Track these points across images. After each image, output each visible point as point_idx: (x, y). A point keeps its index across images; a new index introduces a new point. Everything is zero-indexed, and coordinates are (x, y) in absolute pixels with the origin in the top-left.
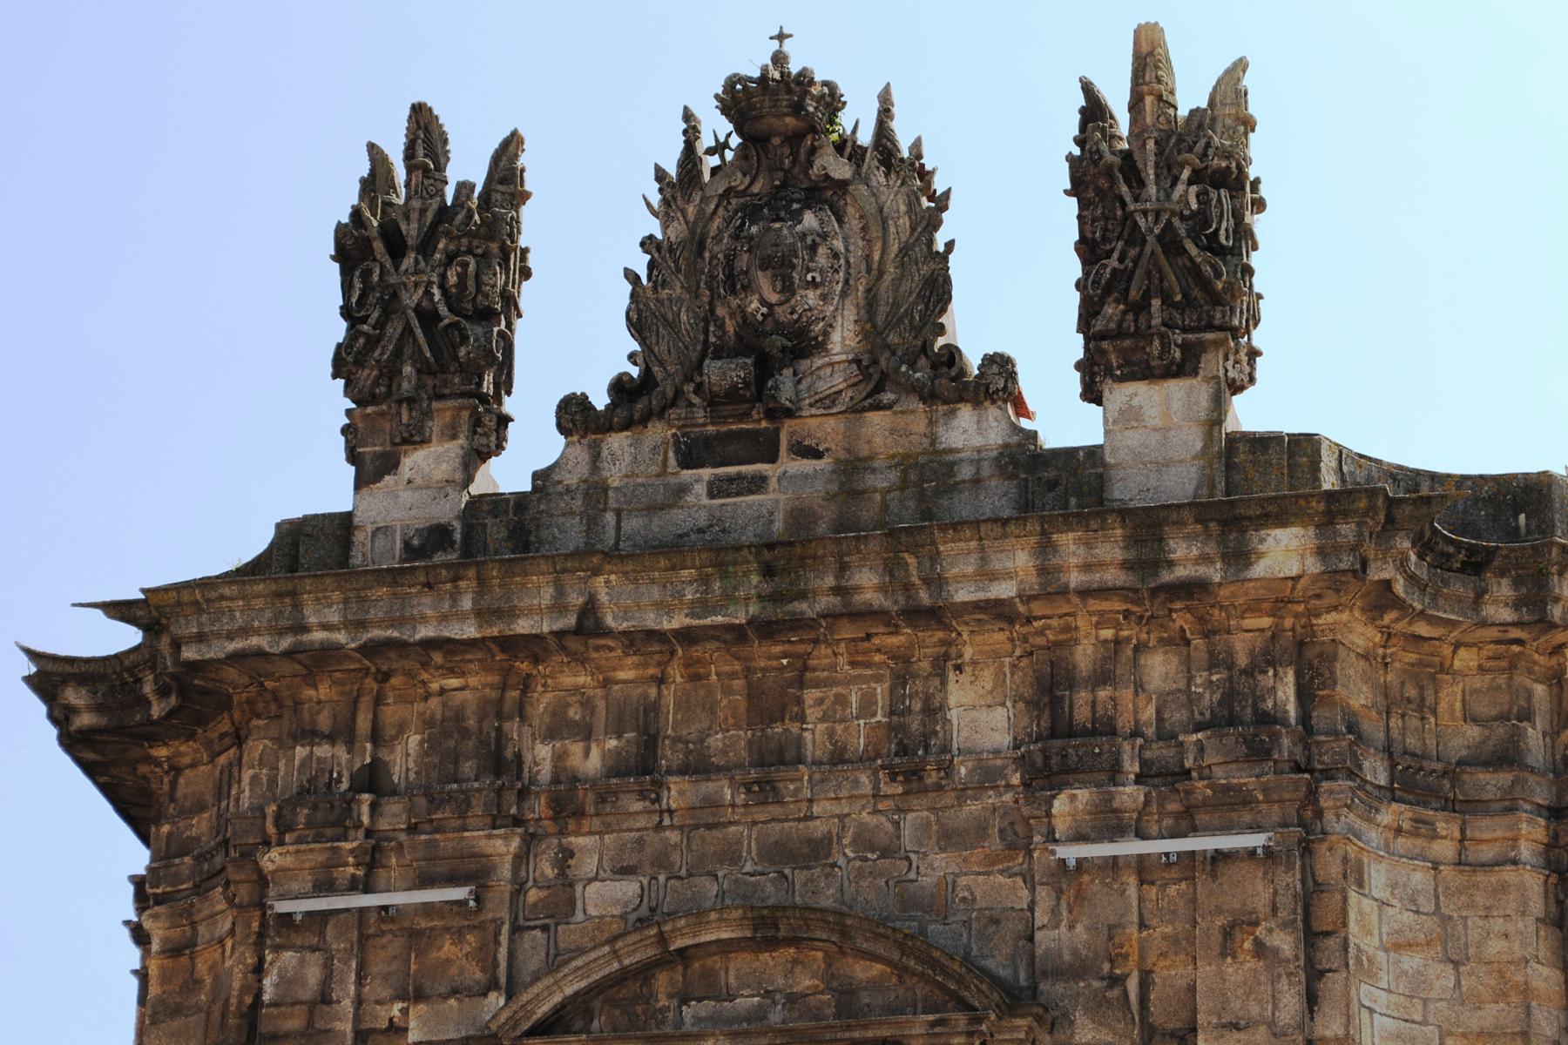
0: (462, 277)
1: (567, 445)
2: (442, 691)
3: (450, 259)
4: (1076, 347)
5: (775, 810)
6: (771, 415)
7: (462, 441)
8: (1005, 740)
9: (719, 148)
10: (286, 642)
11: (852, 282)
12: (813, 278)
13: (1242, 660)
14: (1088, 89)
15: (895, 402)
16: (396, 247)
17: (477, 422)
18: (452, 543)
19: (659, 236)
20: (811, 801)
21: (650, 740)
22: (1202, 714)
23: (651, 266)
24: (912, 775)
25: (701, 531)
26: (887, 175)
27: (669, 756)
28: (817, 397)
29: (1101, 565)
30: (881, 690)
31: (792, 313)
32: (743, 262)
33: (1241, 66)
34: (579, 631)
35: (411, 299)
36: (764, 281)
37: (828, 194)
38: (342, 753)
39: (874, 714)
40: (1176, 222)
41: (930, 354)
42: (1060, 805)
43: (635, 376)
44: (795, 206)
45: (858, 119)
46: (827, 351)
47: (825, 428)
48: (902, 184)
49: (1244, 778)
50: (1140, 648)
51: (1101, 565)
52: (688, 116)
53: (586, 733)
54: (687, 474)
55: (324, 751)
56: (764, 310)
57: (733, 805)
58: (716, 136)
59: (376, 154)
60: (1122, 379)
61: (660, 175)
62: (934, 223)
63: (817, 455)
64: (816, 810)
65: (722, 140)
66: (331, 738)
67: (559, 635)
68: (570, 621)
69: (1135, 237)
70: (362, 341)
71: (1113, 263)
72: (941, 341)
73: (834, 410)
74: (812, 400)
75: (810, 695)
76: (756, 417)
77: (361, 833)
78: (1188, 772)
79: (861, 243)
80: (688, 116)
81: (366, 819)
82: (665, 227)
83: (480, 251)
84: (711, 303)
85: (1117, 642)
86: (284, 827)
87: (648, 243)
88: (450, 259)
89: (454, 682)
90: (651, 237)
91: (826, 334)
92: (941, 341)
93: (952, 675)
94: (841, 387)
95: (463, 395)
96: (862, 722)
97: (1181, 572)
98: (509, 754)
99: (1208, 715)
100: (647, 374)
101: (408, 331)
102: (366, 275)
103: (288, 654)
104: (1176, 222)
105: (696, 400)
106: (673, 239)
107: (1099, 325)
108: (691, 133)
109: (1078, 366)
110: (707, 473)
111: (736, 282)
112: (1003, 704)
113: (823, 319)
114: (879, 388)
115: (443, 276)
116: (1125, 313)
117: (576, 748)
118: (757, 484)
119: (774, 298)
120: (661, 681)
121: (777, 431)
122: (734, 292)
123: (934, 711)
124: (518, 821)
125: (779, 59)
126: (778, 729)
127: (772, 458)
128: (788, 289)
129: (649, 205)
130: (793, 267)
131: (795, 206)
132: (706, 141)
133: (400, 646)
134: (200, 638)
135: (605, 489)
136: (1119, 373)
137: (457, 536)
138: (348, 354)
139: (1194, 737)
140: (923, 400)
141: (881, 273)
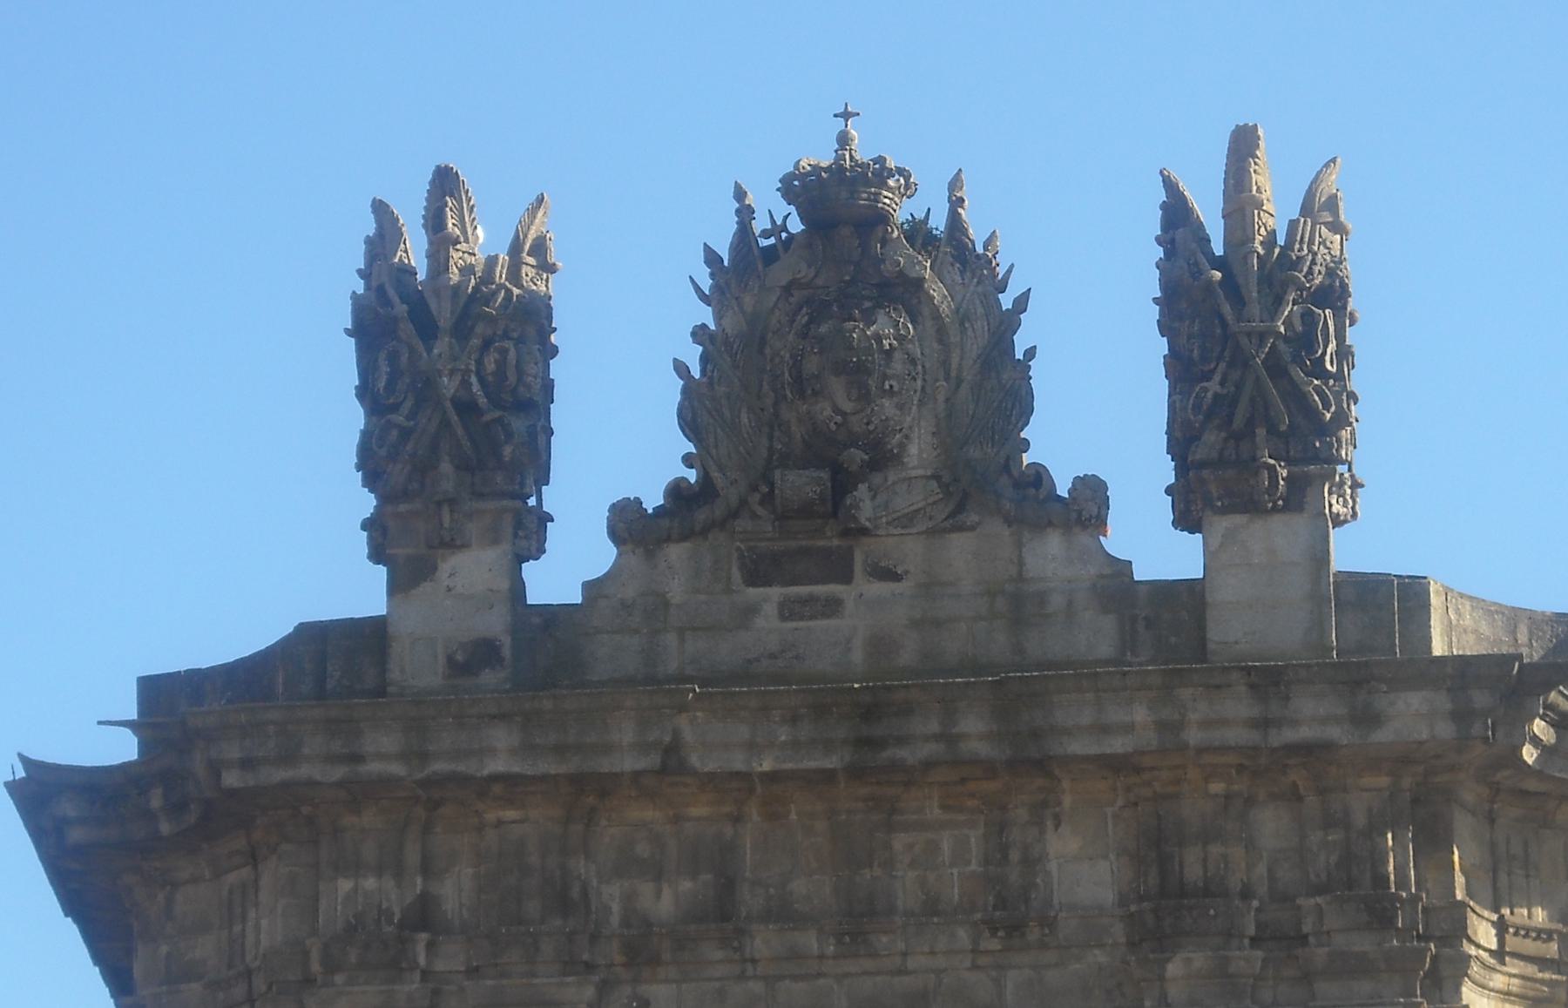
0: (502, 364)
1: (620, 555)
2: (500, 823)
3: (487, 344)
4: (1166, 472)
5: (868, 964)
6: (846, 533)
7: (506, 546)
8: (1108, 896)
9: (776, 229)
10: (339, 772)
11: (928, 390)
12: (891, 386)
13: (1360, 819)
14: (1170, 185)
15: (978, 524)
16: (427, 328)
17: (519, 525)
18: (501, 660)
19: (713, 327)
20: (905, 954)
21: (727, 885)
22: (1318, 876)
23: (705, 359)
24: (1015, 928)
25: (773, 656)
26: (962, 273)
27: (750, 900)
28: (895, 516)
29: (1224, 722)
30: (975, 837)
31: (868, 424)
32: (811, 365)
34: (663, 771)
36: (838, 388)
38: (389, 883)
39: (969, 863)
40: (1282, 346)
41: (1015, 473)
42: (1174, 969)
43: (693, 481)
44: (867, 304)
46: (903, 463)
47: (909, 550)
48: (978, 283)
49: (1363, 944)
50: (1250, 801)
51: (1224, 722)
52: (740, 194)
53: (657, 872)
54: (754, 592)
55: (370, 883)
56: (839, 419)
57: (821, 957)
58: (771, 216)
59: (381, 209)
60: (1224, 511)
61: (711, 258)
62: (1010, 322)
63: (894, 577)
64: (911, 963)
65: (779, 222)
66: (379, 871)
67: (637, 775)
68: (652, 761)
69: (1240, 361)
70: (395, 433)
71: (1213, 386)
73: (914, 530)
74: (890, 519)
75: (899, 841)
76: (829, 534)
77: (417, 976)
78: (1305, 937)
79: (935, 345)
80: (740, 194)
81: (422, 960)
82: (718, 317)
83: (515, 335)
84: (776, 404)
85: (1228, 797)
86: (332, 966)
87: (699, 333)
88: (487, 344)
89: (511, 814)
90: (704, 326)
91: (902, 446)
92: (1027, 459)
93: (1050, 824)
94: (920, 505)
95: (503, 495)
96: (955, 871)
97: (1305, 733)
98: (575, 892)
99: (1324, 876)
100: (705, 478)
101: (445, 424)
102: (393, 357)
103: (340, 784)
104: (1282, 346)
105: (760, 511)
106: (729, 331)
107: (1198, 453)
108: (745, 214)
109: (1169, 491)
110: (776, 592)
111: (803, 386)
112: (1106, 857)
113: (901, 430)
114: (960, 508)
115: (479, 362)
116: (1226, 440)
117: (646, 889)
118: (832, 607)
119: (848, 406)
120: (737, 819)
121: (850, 551)
122: (802, 394)
123: (1032, 862)
124: (590, 967)
125: (844, 140)
126: (867, 873)
127: (847, 578)
128: (865, 397)
129: (698, 289)
130: (869, 373)
131: (867, 304)
132: (760, 224)
133: (462, 780)
135: (666, 604)
136: (1219, 504)
137: (507, 652)
138: (380, 447)
139: (1312, 901)
140: (1009, 521)
141: (959, 381)
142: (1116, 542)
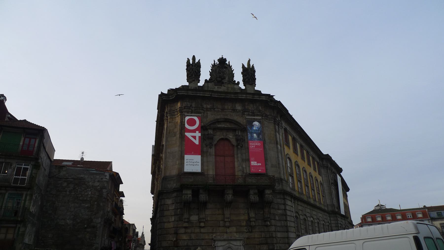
9: (217, 63)
33: (253, 64)
35: (194, 70)
37: (226, 68)
45: (227, 62)
52: (214, 60)
54: (215, 86)
55: (187, 103)
59: (188, 59)
61: (212, 64)
72: (234, 80)
108: (214, 61)
110: (217, 87)
114: (230, 82)
118: (221, 88)
127: (222, 86)
134: (180, 93)
142: (240, 86)
